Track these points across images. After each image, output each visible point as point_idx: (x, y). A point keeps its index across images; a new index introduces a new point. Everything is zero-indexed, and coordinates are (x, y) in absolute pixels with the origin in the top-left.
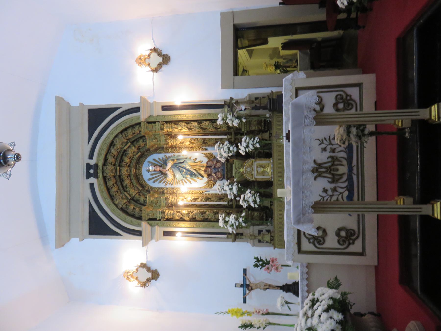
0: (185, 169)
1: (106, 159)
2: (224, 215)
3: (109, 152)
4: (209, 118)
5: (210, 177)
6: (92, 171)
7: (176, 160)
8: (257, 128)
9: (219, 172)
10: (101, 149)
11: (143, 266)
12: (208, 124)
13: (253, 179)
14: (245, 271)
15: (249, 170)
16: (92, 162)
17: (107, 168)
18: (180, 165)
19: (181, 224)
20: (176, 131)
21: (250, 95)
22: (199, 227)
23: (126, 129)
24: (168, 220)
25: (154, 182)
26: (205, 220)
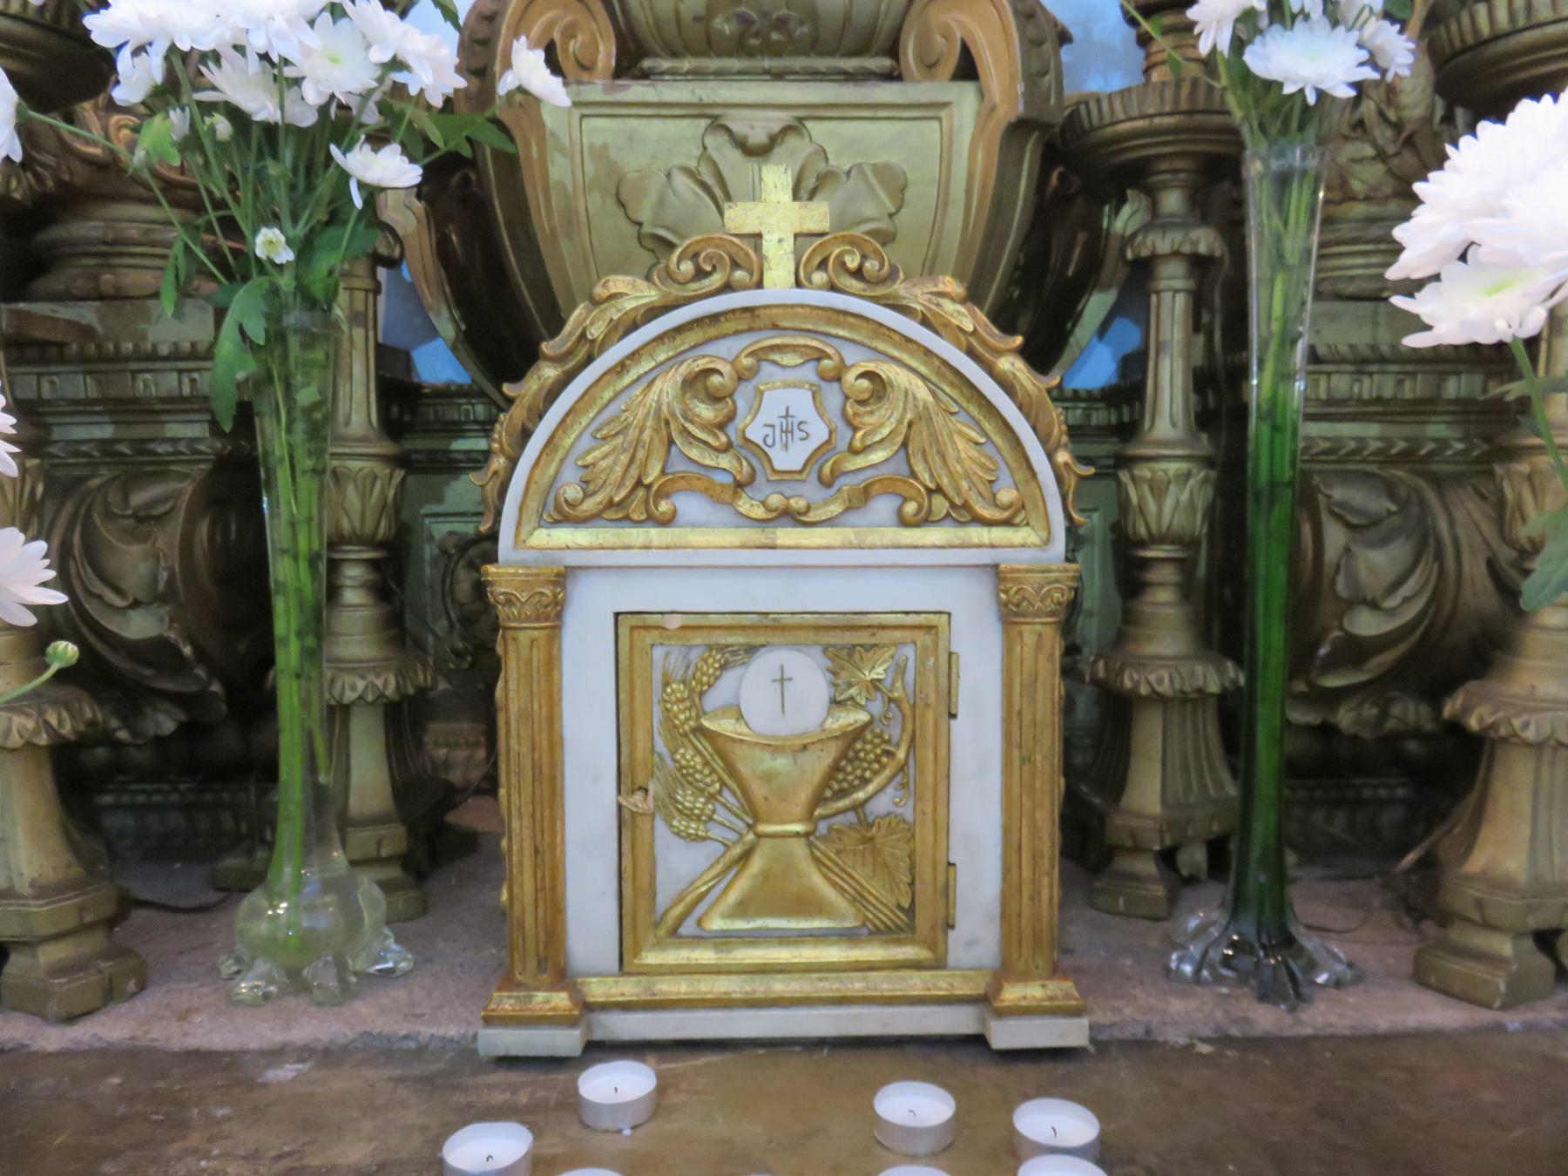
15: (786, 412)
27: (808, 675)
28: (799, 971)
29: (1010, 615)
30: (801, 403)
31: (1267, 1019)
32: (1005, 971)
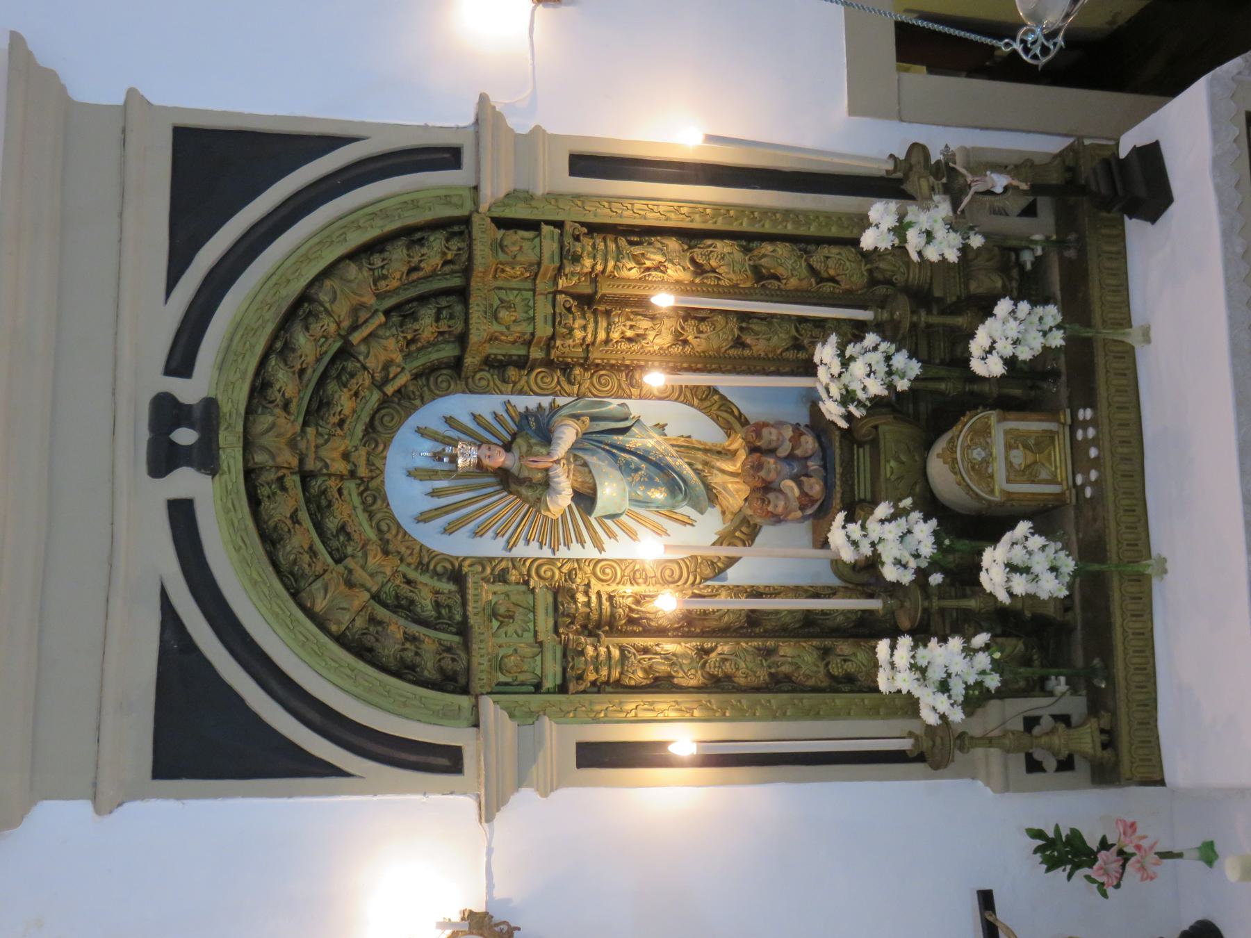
0: (643, 458)
2: (905, 642)
3: (279, 346)
4: (790, 229)
5: (771, 496)
6: (185, 436)
7: (587, 419)
10: (239, 327)
11: (476, 921)
13: (997, 497)
14: (986, 899)
16: (189, 391)
17: (273, 425)
18: (619, 439)
19: (664, 704)
20: (635, 273)
24: (598, 687)
25: (449, 530)
26: (779, 683)
27: (1014, 453)
28: (1060, 454)
29: (1005, 419)
31: (1064, 378)
32: (1058, 421)
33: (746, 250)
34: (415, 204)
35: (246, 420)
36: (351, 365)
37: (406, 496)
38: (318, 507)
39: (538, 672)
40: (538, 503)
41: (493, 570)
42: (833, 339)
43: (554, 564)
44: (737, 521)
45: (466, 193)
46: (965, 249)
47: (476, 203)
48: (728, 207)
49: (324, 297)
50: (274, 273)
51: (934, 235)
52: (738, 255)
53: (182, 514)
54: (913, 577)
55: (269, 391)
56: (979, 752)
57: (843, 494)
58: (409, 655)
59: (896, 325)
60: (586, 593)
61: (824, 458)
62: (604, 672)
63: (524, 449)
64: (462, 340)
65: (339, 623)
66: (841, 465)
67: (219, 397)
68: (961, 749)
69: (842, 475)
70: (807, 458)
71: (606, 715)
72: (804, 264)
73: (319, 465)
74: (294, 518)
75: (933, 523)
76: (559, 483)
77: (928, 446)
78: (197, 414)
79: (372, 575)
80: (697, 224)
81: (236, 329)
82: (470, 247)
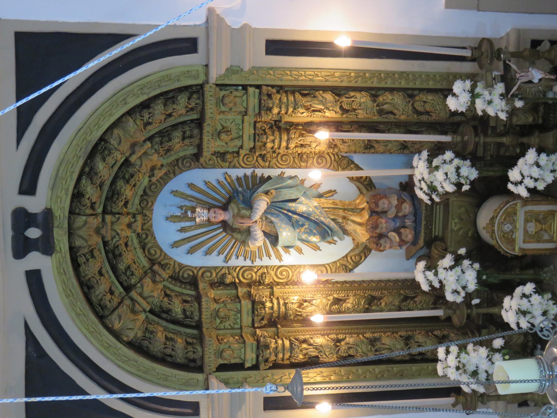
0: (307, 218)
1: (77, 196)
2: (454, 349)
3: (87, 171)
4: (403, 84)
5: (382, 241)
6: (34, 233)
8: (531, 119)
9: (404, 227)
12: (397, 99)
13: (517, 252)
16: (34, 204)
17: (86, 223)
18: (292, 205)
21: (519, 33)
22: (365, 379)
23: (145, 105)
24: (276, 366)
25: (191, 251)
27: (530, 224)
30: (506, 226)
33: (374, 97)
34: (168, 78)
35: (69, 217)
36: (131, 170)
37: (165, 233)
38: (113, 255)
39: (243, 357)
40: (244, 243)
41: (217, 274)
42: (425, 154)
43: (252, 270)
44: (361, 249)
45: (202, 70)
46: (513, 112)
47: (207, 74)
48: (365, 72)
49: (113, 142)
50: (82, 128)
51: (493, 104)
52: (370, 103)
53: (34, 279)
54: (463, 300)
55: (83, 200)
56: (492, 403)
57: (425, 237)
58: (169, 351)
59: (465, 144)
60: (271, 301)
61: (415, 215)
62: (280, 356)
63: (236, 211)
64: (200, 147)
65: (127, 336)
66: (425, 220)
67: (53, 207)
68: (483, 403)
69: (425, 225)
70: (405, 216)
71: (281, 381)
72: (410, 108)
73: (114, 234)
74: (100, 273)
75: (477, 266)
76: (256, 235)
77: (479, 206)
78: (40, 219)
79: (144, 299)
80: (344, 84)
81: (61, 164)
82: (203, 102)
